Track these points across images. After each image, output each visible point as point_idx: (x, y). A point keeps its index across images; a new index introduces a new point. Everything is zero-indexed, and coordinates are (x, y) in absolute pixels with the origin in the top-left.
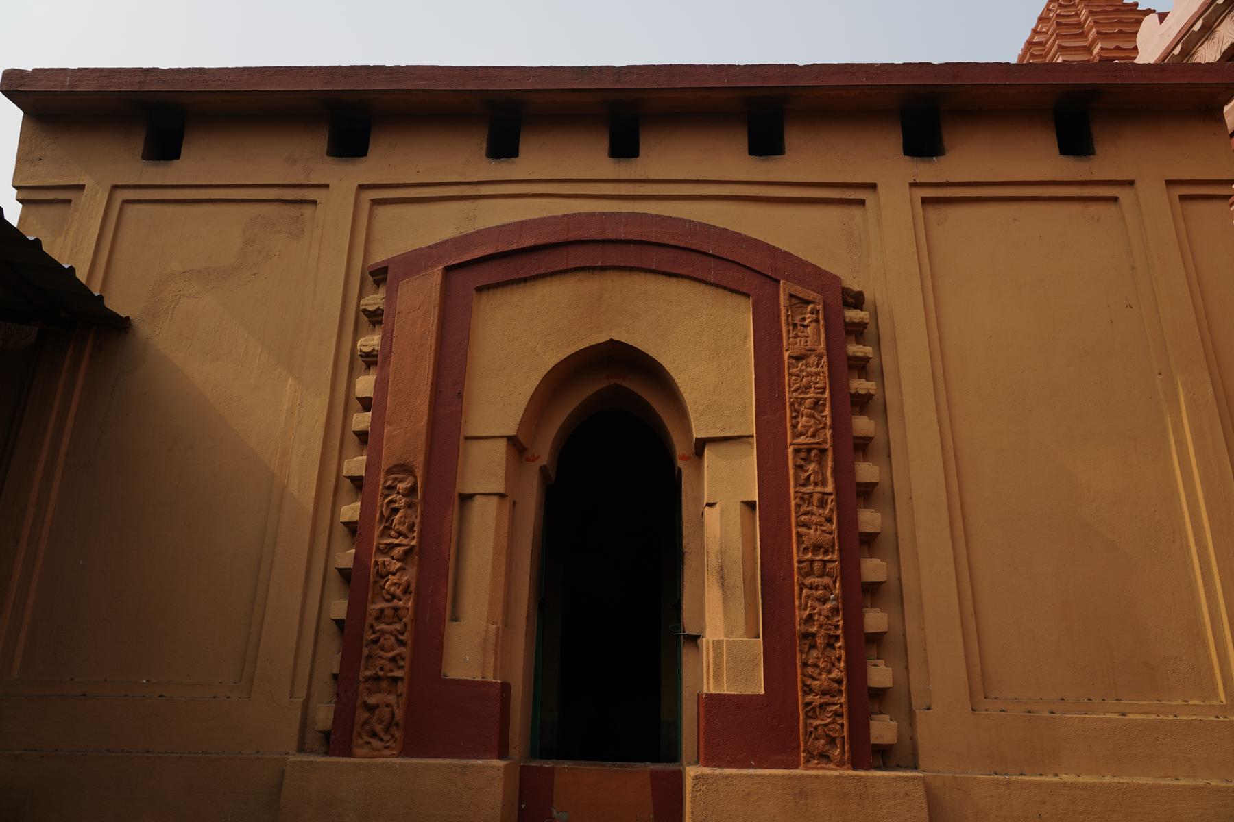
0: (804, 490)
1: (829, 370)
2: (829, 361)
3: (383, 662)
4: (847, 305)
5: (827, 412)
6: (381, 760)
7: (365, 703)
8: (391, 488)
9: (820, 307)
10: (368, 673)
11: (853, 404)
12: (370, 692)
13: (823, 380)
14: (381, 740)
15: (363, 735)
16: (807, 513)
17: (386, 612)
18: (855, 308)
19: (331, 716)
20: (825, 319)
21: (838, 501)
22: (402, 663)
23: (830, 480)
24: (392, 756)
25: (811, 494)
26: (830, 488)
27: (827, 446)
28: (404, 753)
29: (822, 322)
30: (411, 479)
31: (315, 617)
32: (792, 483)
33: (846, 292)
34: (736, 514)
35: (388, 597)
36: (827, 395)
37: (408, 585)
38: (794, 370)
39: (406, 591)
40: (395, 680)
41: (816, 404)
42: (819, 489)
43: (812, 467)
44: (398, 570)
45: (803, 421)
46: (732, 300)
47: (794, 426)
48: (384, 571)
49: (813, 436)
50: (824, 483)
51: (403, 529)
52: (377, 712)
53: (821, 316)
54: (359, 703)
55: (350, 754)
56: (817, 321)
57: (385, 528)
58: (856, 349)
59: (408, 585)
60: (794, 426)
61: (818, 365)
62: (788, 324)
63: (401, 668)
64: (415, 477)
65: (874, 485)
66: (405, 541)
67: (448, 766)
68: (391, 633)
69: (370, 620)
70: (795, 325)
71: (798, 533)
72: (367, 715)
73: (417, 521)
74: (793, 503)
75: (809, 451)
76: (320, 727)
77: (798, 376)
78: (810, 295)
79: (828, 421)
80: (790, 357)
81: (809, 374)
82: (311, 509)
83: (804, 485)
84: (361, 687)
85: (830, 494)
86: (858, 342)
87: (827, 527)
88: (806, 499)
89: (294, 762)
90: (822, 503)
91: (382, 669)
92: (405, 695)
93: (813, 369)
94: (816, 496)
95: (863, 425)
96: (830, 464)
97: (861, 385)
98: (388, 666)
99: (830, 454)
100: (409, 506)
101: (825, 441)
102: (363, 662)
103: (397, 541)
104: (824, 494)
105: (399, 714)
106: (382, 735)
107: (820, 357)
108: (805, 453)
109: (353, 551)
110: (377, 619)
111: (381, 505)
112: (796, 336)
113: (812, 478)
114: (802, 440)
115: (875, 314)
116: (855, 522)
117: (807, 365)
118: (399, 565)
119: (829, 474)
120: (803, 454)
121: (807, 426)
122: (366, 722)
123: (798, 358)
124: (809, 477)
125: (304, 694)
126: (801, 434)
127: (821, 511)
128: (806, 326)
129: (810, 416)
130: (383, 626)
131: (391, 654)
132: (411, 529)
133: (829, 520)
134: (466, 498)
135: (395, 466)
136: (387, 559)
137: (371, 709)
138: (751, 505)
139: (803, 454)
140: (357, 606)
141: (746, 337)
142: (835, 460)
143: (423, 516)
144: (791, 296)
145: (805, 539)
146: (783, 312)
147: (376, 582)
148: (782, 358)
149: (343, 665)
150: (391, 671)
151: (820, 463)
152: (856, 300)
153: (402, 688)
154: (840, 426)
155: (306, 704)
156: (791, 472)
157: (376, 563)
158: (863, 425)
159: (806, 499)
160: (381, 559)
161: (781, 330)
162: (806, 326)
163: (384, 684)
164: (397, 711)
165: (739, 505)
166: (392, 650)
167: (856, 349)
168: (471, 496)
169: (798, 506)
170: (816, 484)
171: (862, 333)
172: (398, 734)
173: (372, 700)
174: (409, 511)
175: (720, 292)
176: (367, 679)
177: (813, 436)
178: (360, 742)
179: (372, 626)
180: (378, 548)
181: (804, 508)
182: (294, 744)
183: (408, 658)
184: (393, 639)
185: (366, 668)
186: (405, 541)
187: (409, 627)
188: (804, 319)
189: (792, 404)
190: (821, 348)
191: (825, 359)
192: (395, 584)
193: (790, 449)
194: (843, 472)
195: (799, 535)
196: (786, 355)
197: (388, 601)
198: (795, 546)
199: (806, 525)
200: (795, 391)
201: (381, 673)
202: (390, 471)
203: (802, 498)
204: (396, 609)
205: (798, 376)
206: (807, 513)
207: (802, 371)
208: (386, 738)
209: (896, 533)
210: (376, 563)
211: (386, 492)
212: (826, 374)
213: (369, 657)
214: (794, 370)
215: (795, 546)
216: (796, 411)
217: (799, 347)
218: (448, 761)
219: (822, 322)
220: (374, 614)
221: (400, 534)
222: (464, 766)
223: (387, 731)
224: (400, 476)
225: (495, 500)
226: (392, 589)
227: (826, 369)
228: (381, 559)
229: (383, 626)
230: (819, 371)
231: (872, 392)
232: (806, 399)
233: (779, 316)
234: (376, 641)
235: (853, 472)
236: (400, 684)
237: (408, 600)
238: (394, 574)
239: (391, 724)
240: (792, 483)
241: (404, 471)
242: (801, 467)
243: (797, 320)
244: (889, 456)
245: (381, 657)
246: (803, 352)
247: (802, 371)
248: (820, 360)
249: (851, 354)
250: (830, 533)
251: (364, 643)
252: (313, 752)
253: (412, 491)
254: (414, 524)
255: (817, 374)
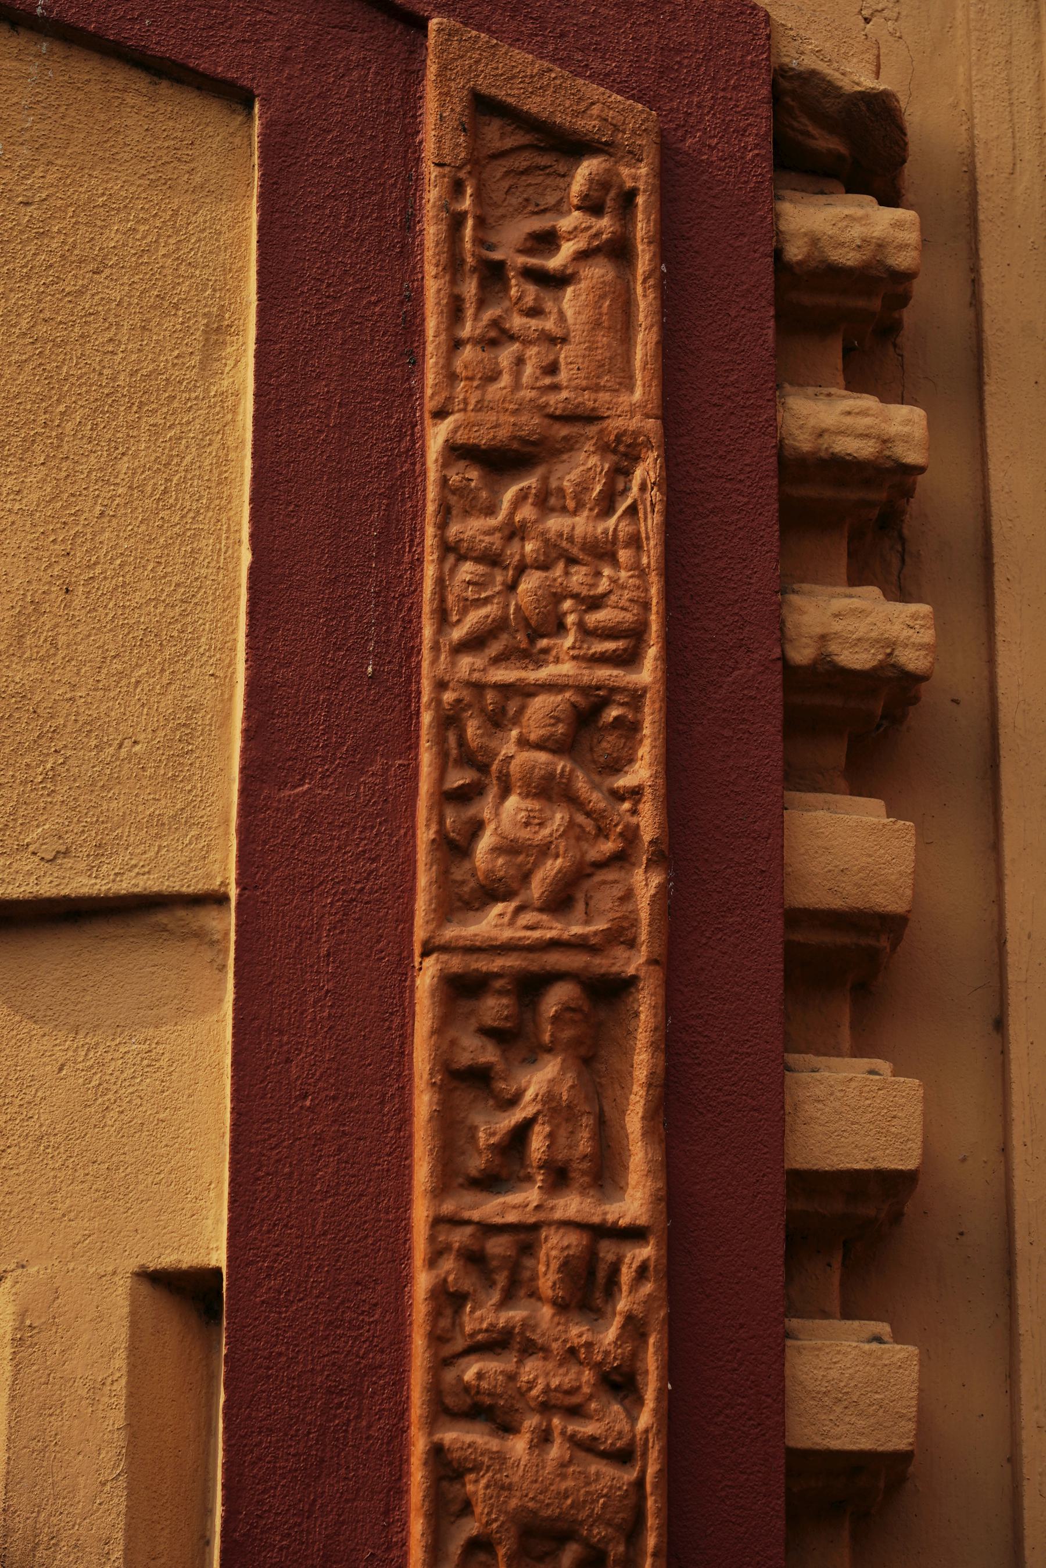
0: (494, 1208)
1: (671, 528)
2: (674, 483)
4: (802, 166)
5: (641, 772)
9: (639, 175)
11: (798, 724)
13: (631, 585)
16: (496, 1343)
18: (855, 185)
20: (667, 242)
21: (677, 1273)
23: (639, 1156)
25: (526, 1235)
26: (633, 1203)
27: (634, 962)
29: (644, 259)
32: (422, 1172)
33: (795, 95)
34: (103, 1337)
36: (647, 673)
38: (470, 528)
41: (588, 725)
42: (572, 1205)
43: (540, 1080)
45: (507, 814)
46: (152, 121)
47: (454, 848)
49: (560, 901)
50: (604, 1172)
53: (642, 227)
56: (619, 251)
58: (837, 418)
60: (454, 848)
61: (607, 504)
62: (454, 266)
65: (894, 1185)
70: (493, 275)
71: (437, 1452)
74: (422, 1281)
75: (530, 987)
77: (492, 560)
78: (592, 104)
79: (648, 822)
80: (455, 452)
81: (558, 554)
83: (490, 1182)
85: (635, 1234)
86: (857, 381)
87: (608, 1420)
88: (495, 1260)
90: (587, 1288)
93: (582, 525)
94: (555, 1246)
95: (849, 845)
96: (642, 1062)
97: (853, 622)
99: (645, 1009)
101: (621, 935)
104: (602, 1232)
107: (623, 455)
108: (505, 1001)
112: (498, 336)
113: (537, 1144)
114: (491, 923)
115: (960, 226)
116: (771, 1391)
117: (546, 501)
119: (634, 1122)
120: (494, 1008)
121: (532, 846)
123: (500, 461)
124: (521, 1133)
126: (491, 892)
127: (577, 1332)
128: (557, 281)
129: (548, 790)
133: (621, 1383)
138: (185, 1291)
139: (494, 1008)
141: (218, 332)
142: (671, 1043)
144: (484, 106)
145: (476, 1487)
146: (432, 195)
148: (415, 453)
151: (593, 1057)
152: (858, 143)
154: (712, 842)
156: (423, 1103)
158: (849, 845)
159: (495, 1260)
161: (415, 298)
162: (557, 281)
165: (119, 1298)
167: (837, 418)
169: (448, 1300)
170: (559, 1177)
171: (888, 330)
175: (87, 71)
177: (560, 901)
181: (483, 1315)
188: (548, 241)
189: (449, 721)
190: (634, 405)
191: (647, 469)
193: (426, 976)
194: (716, 1111)
195: (446, 1468)
196: (437, 437)
198: (417, 1526)
199: (492, 1412)
200: (474, 643)
203: (474, 1259)
205: (492, 560)
206: (496, 1343)
207: (515, 532)
209: (1014, 1460)
212: (651, 555)
214: (470, 528)
215: (417, 1526)
216: (468, 758)
217: (504, 397)
219: (644, 259)
227: (651, 524)
230: (607, 540)
231: (912, 660)
232: (527, 691)
233: (410, 222)
235: (772, 1115)
240: (422, 1172)
242: (478, 1078)
243: (508, 249)
244: (1000, 1024)
246: (531, 423)
247: (515, 532)
248: (621, 471)
249: (803, 442)
250: (623, 1456)
255: (602, 552)
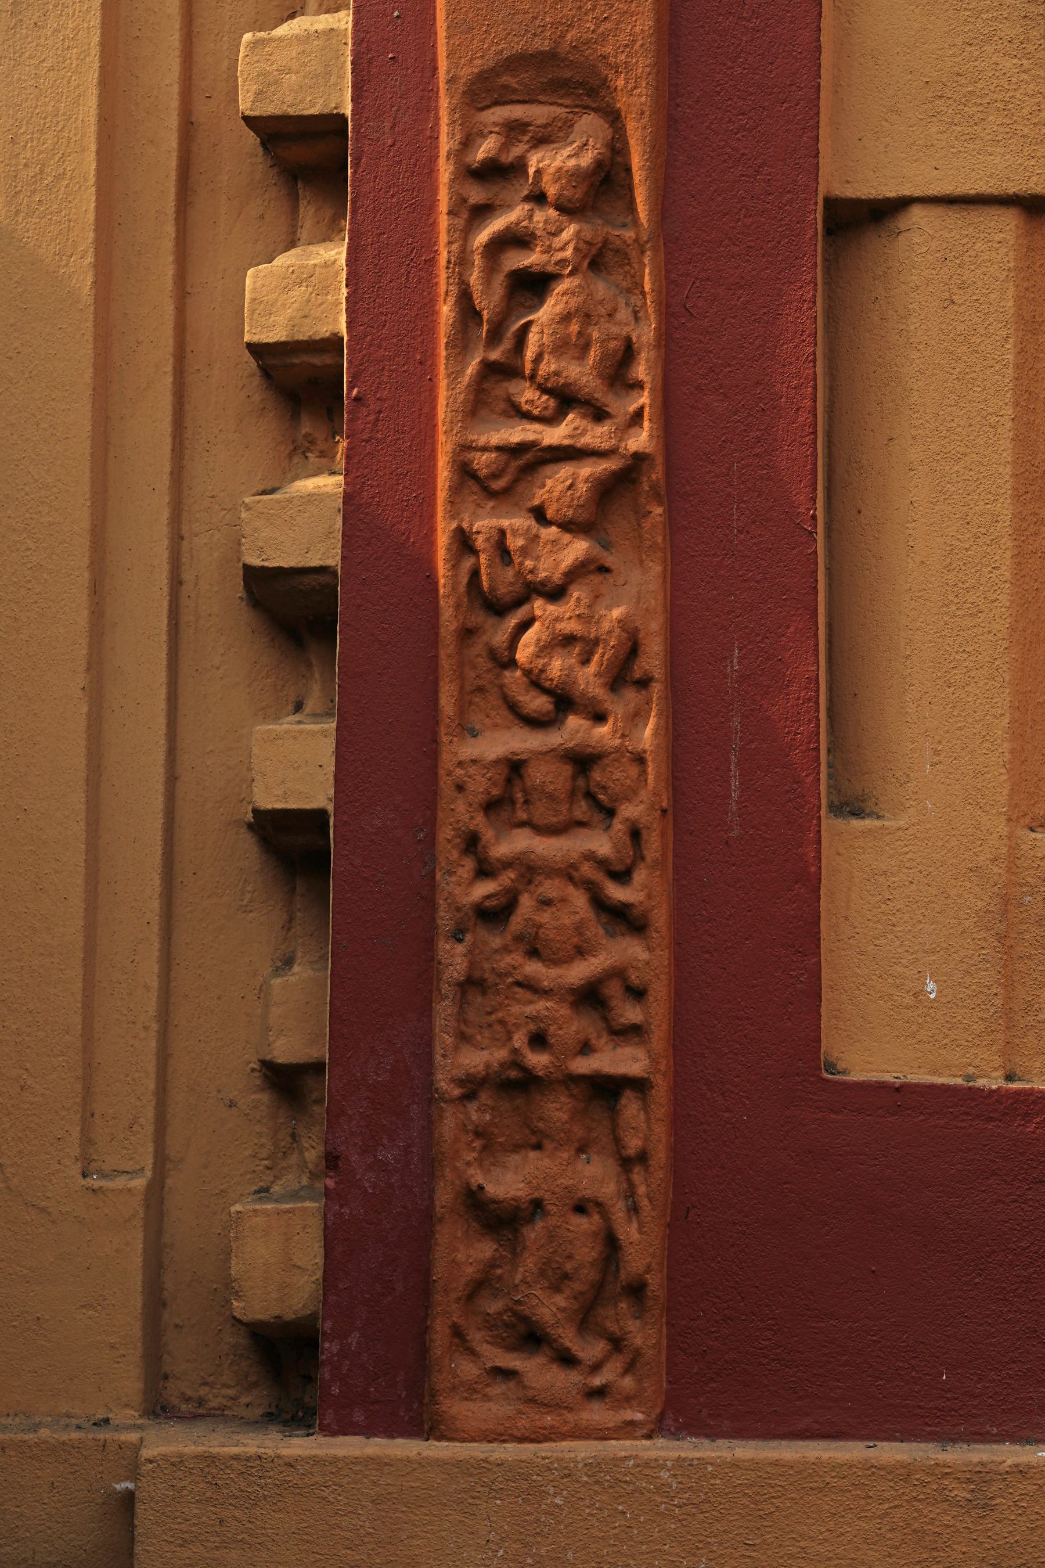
3: (541, 1006)
6: (584, 1450)
7: (474, 1201)
8: (497, 172)
10: (476, 1060)
12: (489, 1144)
14: (567, 1360)
15: (477, 1337)
17: (538, 775)
19: (310, 1254)
22: (631, 1014)
24: (627, 1430)
28: (678, 1416)
30: (590, 127)
31: (158, 802)
35: (538, 703)
37: (633, 650)
39: (622, 674)
40: (607, 1089)
44: (577, 572)
48: (500, 581)
51: (581, 373)
52: (533, 1233)
54: (444, 1196)
55: (426, 1425)
57: (491, 370)
59: (633, 650)
63: (634, 1032)
64: (614, 118)
66: (596, 436)
67: (905, 1473)
68: (568, 873)
69: (459, 813)
72: (485, 1249)
73: (646, 333)
76: (258, 1304)
82: (85, 283)
84: (449, 1124)
89: (178, 1462)
91: (539, 1040)
92: (660, 1155)
98: (571, 1025)
100: (596, 260)
102: (444, 1010)
103: (554, 435)
105: (641, 1245)
106: (568, 1338)
109: (329, 484)
110: (491, 807)
111: (454, 255)
118: (578, 548)
122: (483, 1284)
125: (149, 1162)
130: (520, 842)
131: (578, 972)
132: (618, 371)
134: (860, 220)
135: (515, 63)
136: (516, 523)
137: (502, 1221)
140: (390, 749)
143: (668, 314)
147: (467, 633)
149: (352, 1008)
150: (586, 1048)
153: (641, 1124)
155: (156, 1194)
157: (464, 542)
160: (484, 524)
163: (556, 1109)
164: (629, 1232)
166: (581, 952)
168: (884, 212)
172: (643, 1334)
173: (507, 1182)
174: (601, 288)
176: (472, 1087)
178: (468, 1369)
179: (472, 843)
180: (465, 472)
182: (131, 1383)
183: (660, 991)
184: (580, 900)
185: (463, 1038)
186: (596, 436)
187: (653, 845)
192: (569, 640)
197: (535, 722)
201: (538, 1061)
202: (483, 91)
204: (582, 761)
208: (590, 1350)
210: (464, 542)
211: (476, 195)
213: (472, 984)
218: (892, 1452)
220: (480, 785)
221: (565, 399)
222: (980, 1477)
223: (585, 1319)
224: (538, 113)
225: (1006, 225)
226: (556, 666)
228: (484, 524)
229: (520, 842)
234: (494, 914)
236: (630, 1107)
237: (637, 716)
238: (556, 593)
239: (609, 1282)
241: (558, 88)
245: (530, 986)
251: (445, 920)
252: (199, 1413)
253: (603, 186)
254: (628, 353)
